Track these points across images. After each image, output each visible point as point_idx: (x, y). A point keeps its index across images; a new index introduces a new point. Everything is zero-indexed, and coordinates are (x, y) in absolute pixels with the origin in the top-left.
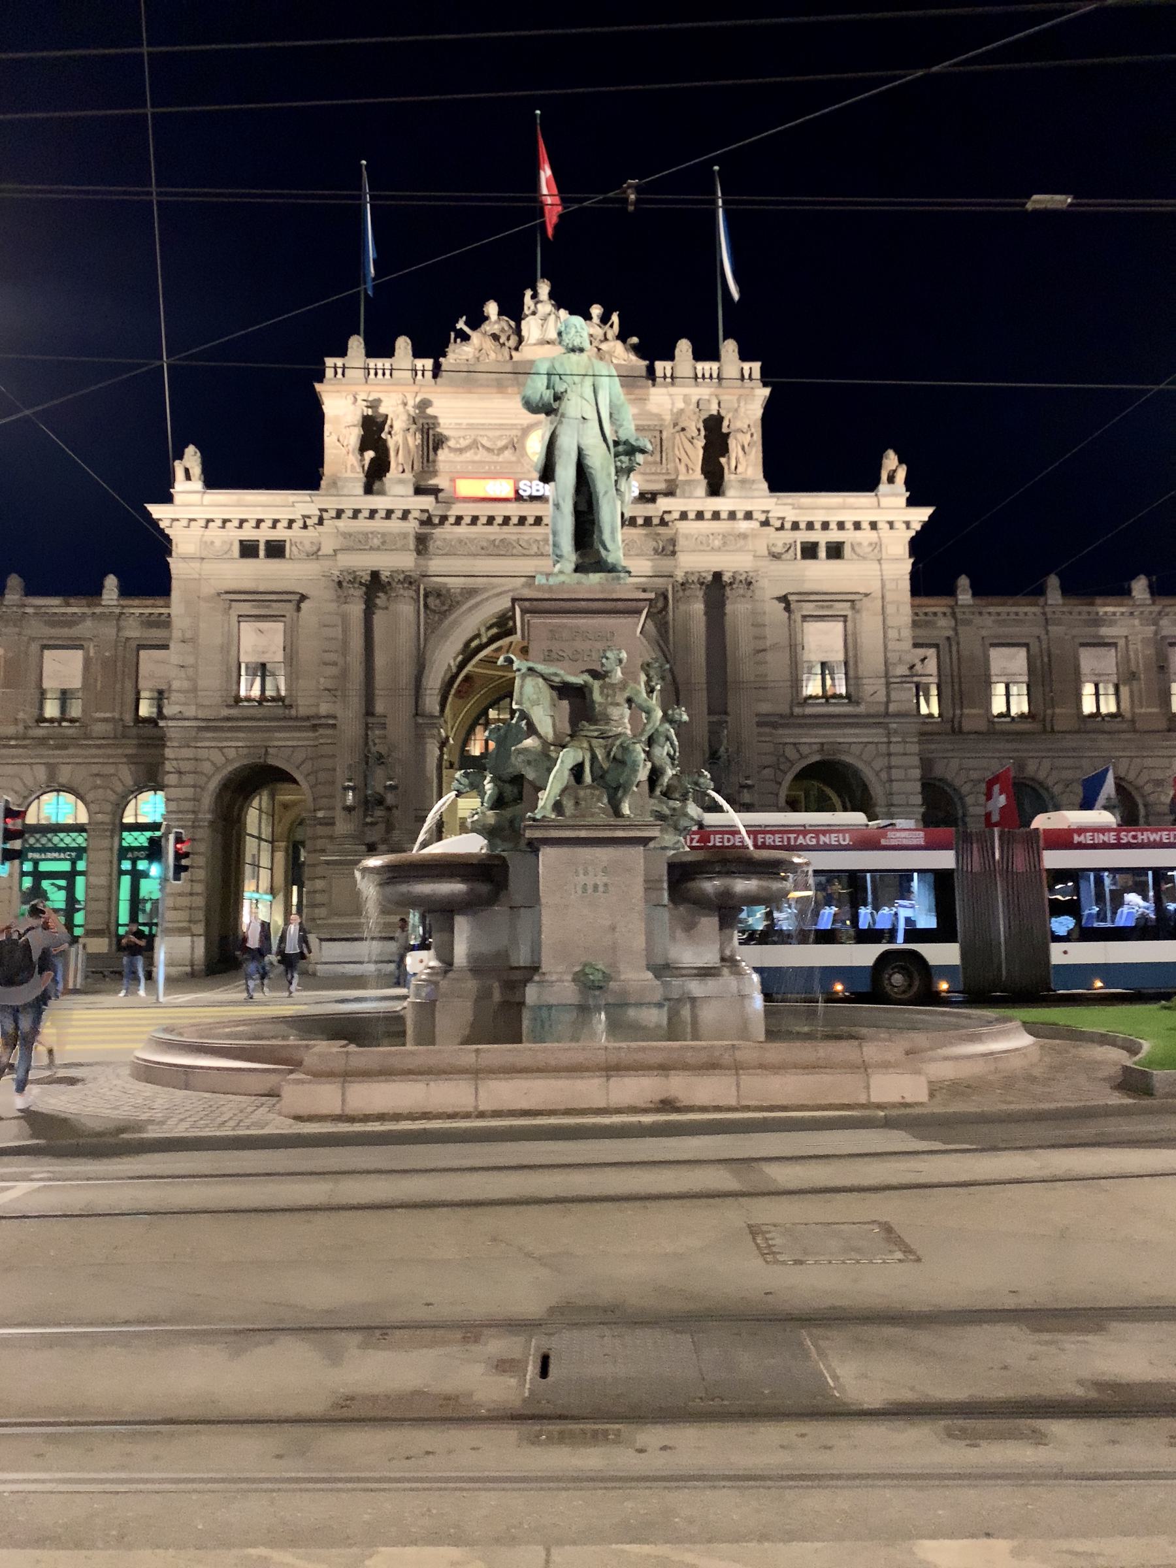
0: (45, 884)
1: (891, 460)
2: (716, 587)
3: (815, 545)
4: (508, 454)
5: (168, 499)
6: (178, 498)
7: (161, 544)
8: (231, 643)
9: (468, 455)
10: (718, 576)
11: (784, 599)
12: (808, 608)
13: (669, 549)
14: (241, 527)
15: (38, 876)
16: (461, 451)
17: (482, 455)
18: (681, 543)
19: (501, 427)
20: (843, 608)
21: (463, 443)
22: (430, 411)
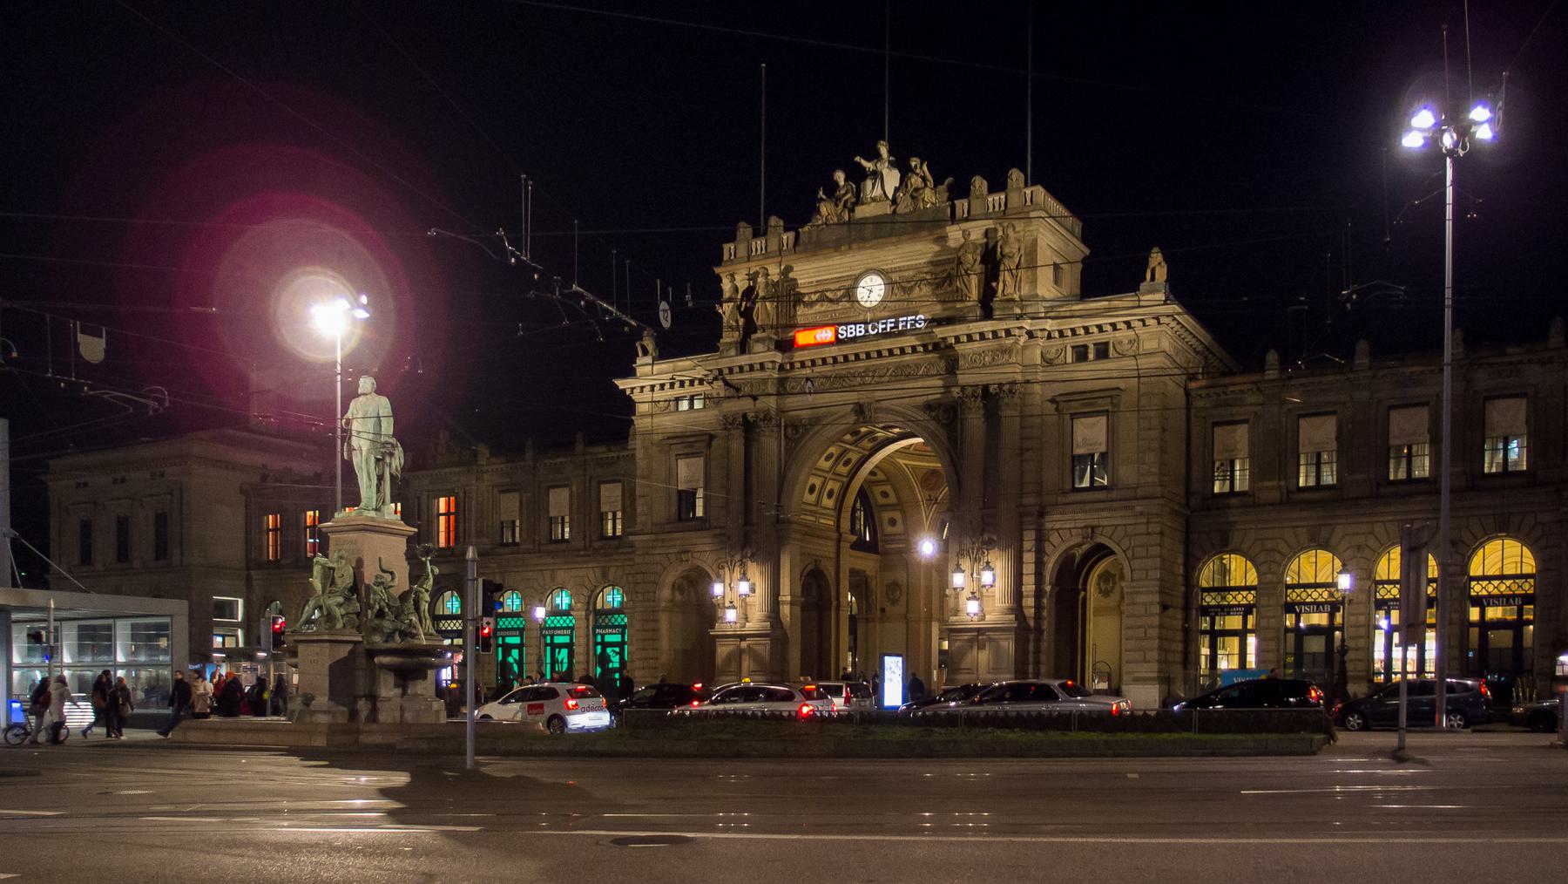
0: (609, 650)
1: (1156, 258)
2: (990, 397)
3: (1086, 347)
4: (844, 304)
5: (631, 373)
6: (639, 371)
7: (628, 405)
8: (671, 475)
9: (818, 308)
10: (986, 387)
11: (1053, 401)
12: (1076, 407)
13: (952, 366)
14: (672, 386)
15: (605, 645)
16: (812, 304)
17: (826, 307)
18: (961, 362)
19: (839, 279)
20: (1104, 404)
21: (814, 297)
22: (791, 275)
